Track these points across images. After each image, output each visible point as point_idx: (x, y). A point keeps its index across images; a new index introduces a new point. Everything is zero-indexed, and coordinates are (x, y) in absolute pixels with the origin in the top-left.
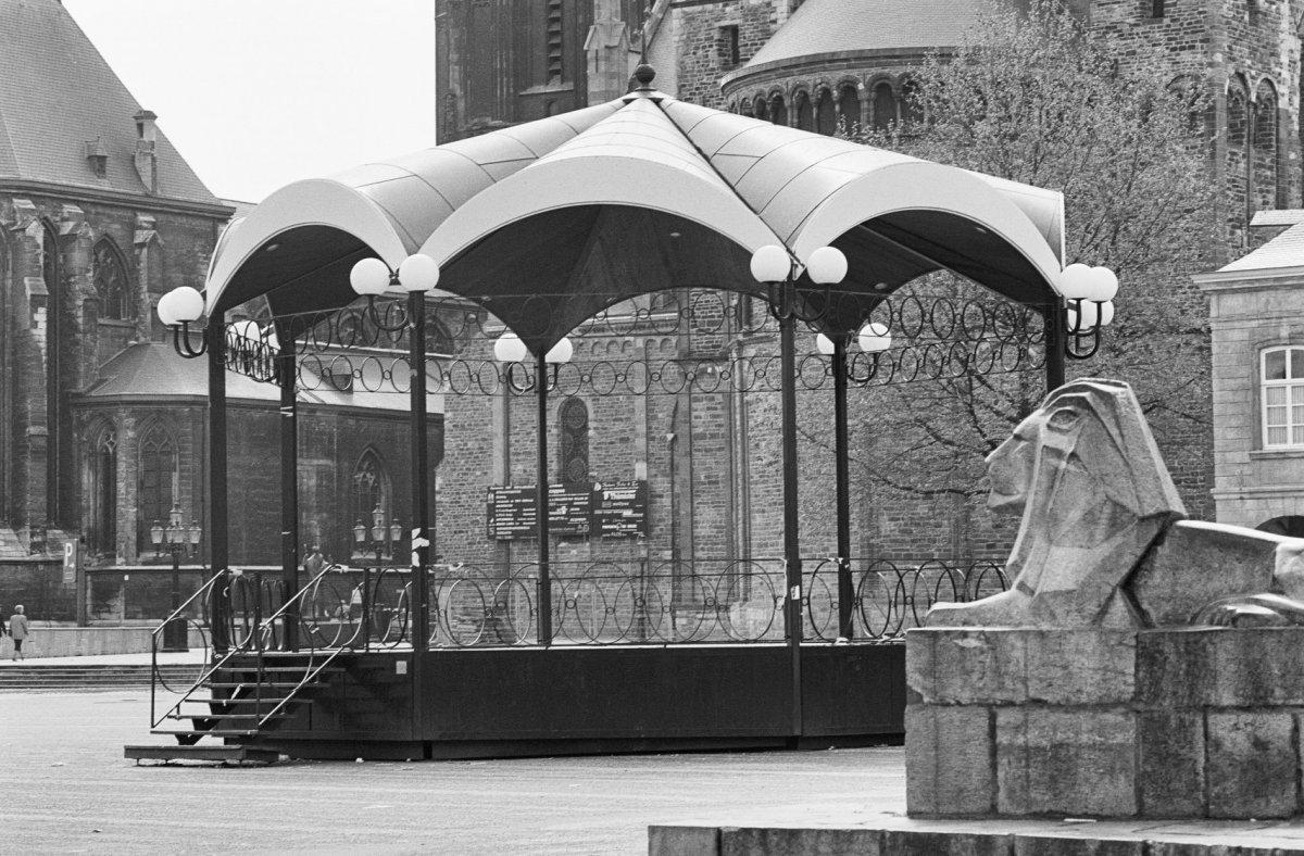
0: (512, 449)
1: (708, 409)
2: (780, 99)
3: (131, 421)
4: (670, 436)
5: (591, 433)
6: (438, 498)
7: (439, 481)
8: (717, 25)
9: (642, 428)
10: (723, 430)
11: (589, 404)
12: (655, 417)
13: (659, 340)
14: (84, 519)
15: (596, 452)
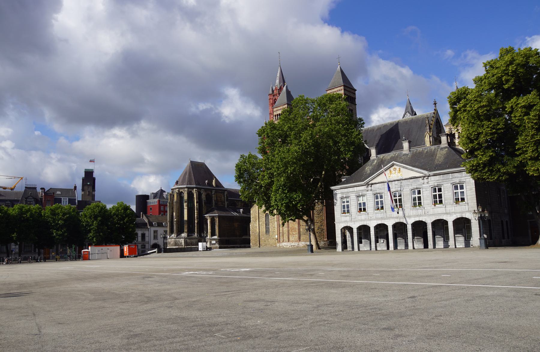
5: (270, 218)
7: (250, 225)
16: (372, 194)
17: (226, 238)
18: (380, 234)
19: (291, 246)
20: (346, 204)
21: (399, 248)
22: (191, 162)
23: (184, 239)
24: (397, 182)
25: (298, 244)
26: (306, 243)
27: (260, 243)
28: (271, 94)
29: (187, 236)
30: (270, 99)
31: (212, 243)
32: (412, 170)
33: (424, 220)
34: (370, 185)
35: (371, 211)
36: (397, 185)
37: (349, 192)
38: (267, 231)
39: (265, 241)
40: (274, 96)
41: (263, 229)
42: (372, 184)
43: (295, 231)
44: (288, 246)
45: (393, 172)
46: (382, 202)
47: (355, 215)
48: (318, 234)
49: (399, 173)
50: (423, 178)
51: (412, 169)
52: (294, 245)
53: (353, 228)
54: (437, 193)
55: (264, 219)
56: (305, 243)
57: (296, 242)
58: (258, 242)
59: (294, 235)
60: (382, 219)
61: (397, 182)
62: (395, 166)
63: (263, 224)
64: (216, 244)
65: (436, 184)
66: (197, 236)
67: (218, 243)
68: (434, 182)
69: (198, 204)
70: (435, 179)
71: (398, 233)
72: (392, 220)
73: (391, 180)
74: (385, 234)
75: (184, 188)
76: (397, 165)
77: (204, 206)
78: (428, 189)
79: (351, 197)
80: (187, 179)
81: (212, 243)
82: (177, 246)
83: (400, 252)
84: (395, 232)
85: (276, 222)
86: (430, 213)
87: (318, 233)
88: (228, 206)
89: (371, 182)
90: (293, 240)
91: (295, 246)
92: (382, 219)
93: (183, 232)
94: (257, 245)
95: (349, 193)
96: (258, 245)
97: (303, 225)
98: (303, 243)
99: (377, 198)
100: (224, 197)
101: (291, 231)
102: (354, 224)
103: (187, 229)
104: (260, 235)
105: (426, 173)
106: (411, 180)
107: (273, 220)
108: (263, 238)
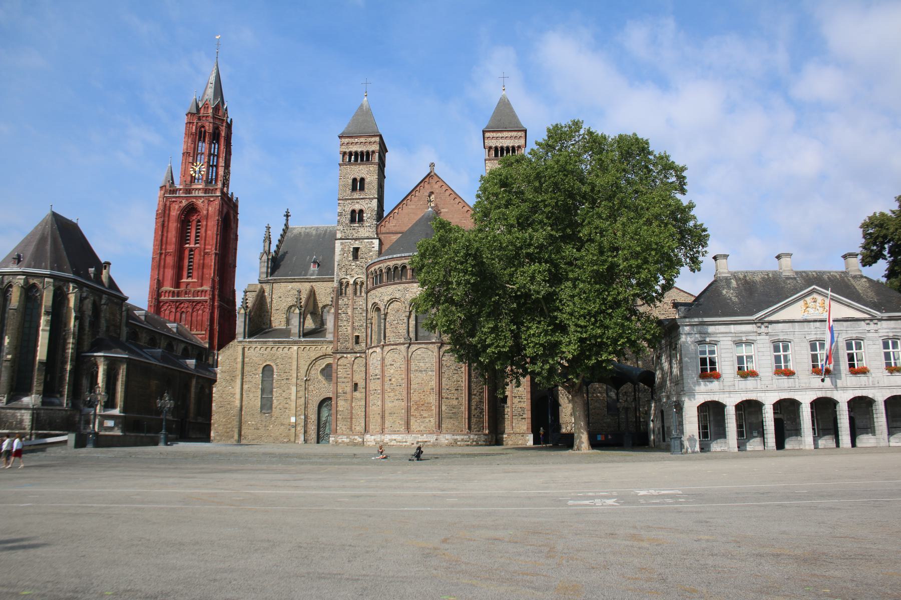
4: (305, 379)
5: (275, 376)
6: (214, 395)
7: (214, 390)
9: (295, 375)
10: (349, 376)
11: (275, 367)
12: (300, 372)
13: (303, 347)
16: (768, 341)
17: (135, 415)
18: (749, 421)
20: (707, 356)
21: (787, 446)
22: (54, 215)
23: (30, 412)
24: (818, 324)
25: (436, 440)
26: (456, 437)
27: (243, 433)
28: (194, 114)
29: (40, 404)
30: (190, 123)
31: (105, 425)
32: (849, 306)
33: (870, 396)
34: (766, 324)
35: (767, 374)
36: (818, 330)
37: (717, 333)
38: (267, 405)
39: (258, 429)
40: (199, 118)
41: (254, 400)
42: (771, 322)
43: (429, 409)
44: (406, 442)
45: (811, 304)
46: (786, 360)
47: (732, 379)
48: (475, 419)
49: (807, 307)
50: (868, 322)
51: (850, 303)
52: (424, 440)
53: (728, 404)
54: (782, 353)
55: (259, 377)
56: (453, 437)
57: (431, 434)
58: (236, 430)
60: (790, 389)
61: (818, 323)
62: (815, 295)
63: (253, 390)
64: (116, 429)
65: (891, 335)
66: (67, 404)
67: (120, 426)
68: (888, 330)
69: (77, 324)
70: (889, 326)
71: (785, 419)
72: (811, 393)
73: (807, 318)
74: (760, 420)
75: (43, 276)
76: (820, 293)
77: (87, 329)
78: (877, 342)
79: (722, 343)
80: (49, 254)
81: (105, 425)
82: (7, 429)
83: (790, 456)
84: (777, 416)
85: (294, 389)
86: (881, 384)
87: (476, 416)
88: (126, 342)
89: (766, 319)
90: (422, 428)
91: (429, 444)
92: (790, 389)
93: (27, 392)
94: (233, 437)
95: (718, 335)
96: (236, 437)
97: (447, 398)
98: (448, 437)
99: (777, 349)
100: (121, 314)
101: (417, 409)
102: (730, 397)
103: (42, 385)
104: (243, 413)
105: (878, 314)
106: (845, 324)
107: (285, 381)
108: (250, 422)
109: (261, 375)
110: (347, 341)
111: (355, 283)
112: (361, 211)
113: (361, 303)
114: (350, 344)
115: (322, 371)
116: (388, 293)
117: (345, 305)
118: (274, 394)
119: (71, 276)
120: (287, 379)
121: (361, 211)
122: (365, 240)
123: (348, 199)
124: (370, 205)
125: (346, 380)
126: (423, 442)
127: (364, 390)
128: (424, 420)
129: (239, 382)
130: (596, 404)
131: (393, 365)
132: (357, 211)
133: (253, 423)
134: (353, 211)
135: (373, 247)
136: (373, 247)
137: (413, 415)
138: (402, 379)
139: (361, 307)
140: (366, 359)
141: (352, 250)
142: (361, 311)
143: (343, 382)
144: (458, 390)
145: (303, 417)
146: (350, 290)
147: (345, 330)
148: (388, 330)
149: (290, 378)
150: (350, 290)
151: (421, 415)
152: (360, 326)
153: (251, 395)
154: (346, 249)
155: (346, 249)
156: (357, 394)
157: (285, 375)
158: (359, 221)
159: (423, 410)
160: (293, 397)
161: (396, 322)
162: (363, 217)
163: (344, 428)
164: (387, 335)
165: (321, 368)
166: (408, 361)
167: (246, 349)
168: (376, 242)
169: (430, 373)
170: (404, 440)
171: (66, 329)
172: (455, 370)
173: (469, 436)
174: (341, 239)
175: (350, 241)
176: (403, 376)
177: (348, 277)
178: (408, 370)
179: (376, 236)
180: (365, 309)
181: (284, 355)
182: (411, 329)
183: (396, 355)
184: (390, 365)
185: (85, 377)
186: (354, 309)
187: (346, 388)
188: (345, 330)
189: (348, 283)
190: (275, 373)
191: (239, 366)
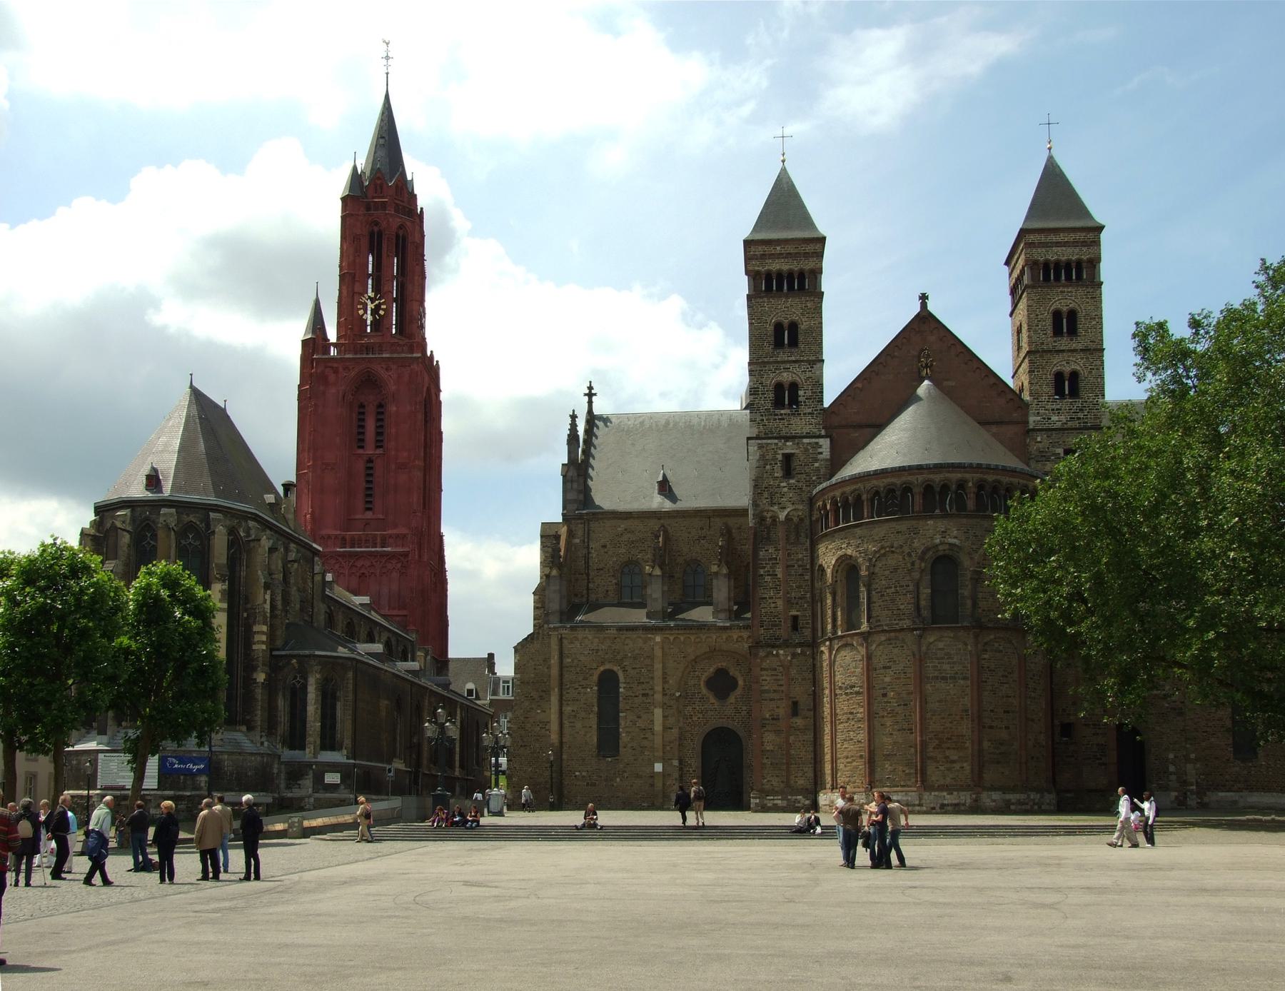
0: (564, 698)
1: (772, 675)
2: (859, 497)
3: (318, 668)
4: (678, 694)
5: (621, 690)
8: (780, 452)
9: (659, 688)
10: (782, 688)
13: (672, 638)
14: (279, 729)
15: (625, 701)
19: (943, 806)
26: (1008, 797)
38: (608, 742)
55: (592, 692)
59: (953, 762)
85: (658, 712)
90: (948, 781)
91: (963, 808)
97: (991, 727)
98: (996, 796)
101: (938, 747)
109: (596, 688)
110: (776, 626)
111: (788, 519)
112: (794, 387)
113: (800, 556)
114: (784, 631)
115: (710, 683)
116: (876, 538)
117: (770, 559)
118: (622, 722)
119: (212, 499)
120: (643, 695)
121: (794, 387)
122: (806, 441)
123: (768, 363)
124: (810, 374)
125: (775, 696)
126: (951, 805)
127: (812, 713)
128: (954, 765)
129: (554, 699)
130: (1213, 739)
131: (890, 667)
132: (786, 386)
133: (584, 774)
134: (779, 387)
135: (821, 453)
136: (821, 453)
137: (931, 758)
138: (908, 694)
139: (800, 563)
140: (814, 659)
141: (780, 457)
142: (800, 571)
143: (771, 700)
144: (1008, 712)
145: (676, 763)
146: (780, 533)
147: (773, 605)
148: (877, 604)
149: (650, 692)
150: (780, 533)
151: (947, 757)
152: (800, 598)
153: (579, 725)
154: (769, 457)
155: (769, 457)
156: (799, 721)
157: (640, 687)
158: (790, 405)
159: (948, 748)
160: (658, 727)
161: (893, 590)
162: (797, 396)
163: (775, 782)
164: (874, 614)
165: (706, 674)
166: (921, 659)
167: (565, 642)
168: (825, 444)
169: (962, 682)
170: (917, 802)
171: (249, 606)
172: (1003, 676)
173: (1029, 796)
174: (757, 438)
175: (776, 441)
176: (911, 688)
177: (775, 508)
178: (921, 679)
179: (823, 432)
180: (808, 567)
181: (637, 652)
182: (923, 603)
183: (896, 651)
184: (884, 668)
185: (280, 694)
186: (788, 566)
187: (777, 710)
188: (773, 605)
189: (774, 518)
190: (621, 685)
191: (555, 671)
